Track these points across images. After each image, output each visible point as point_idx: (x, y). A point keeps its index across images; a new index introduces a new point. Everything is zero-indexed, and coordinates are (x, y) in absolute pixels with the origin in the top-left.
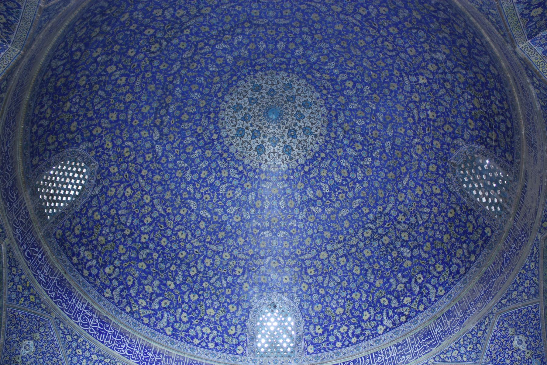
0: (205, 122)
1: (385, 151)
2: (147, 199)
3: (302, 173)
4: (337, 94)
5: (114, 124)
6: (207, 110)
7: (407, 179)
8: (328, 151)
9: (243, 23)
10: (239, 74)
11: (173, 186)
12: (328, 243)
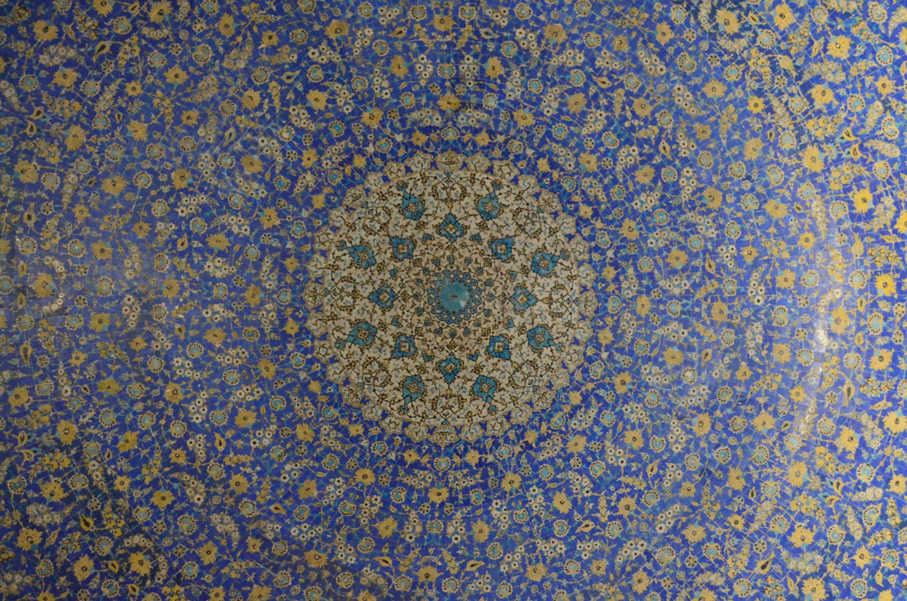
3: (599, 224)
4: (357, 129)
6: (389, 469)
8: (530, 152)
9: (132, 353)
10: (303, 375)
12: (775, 145)
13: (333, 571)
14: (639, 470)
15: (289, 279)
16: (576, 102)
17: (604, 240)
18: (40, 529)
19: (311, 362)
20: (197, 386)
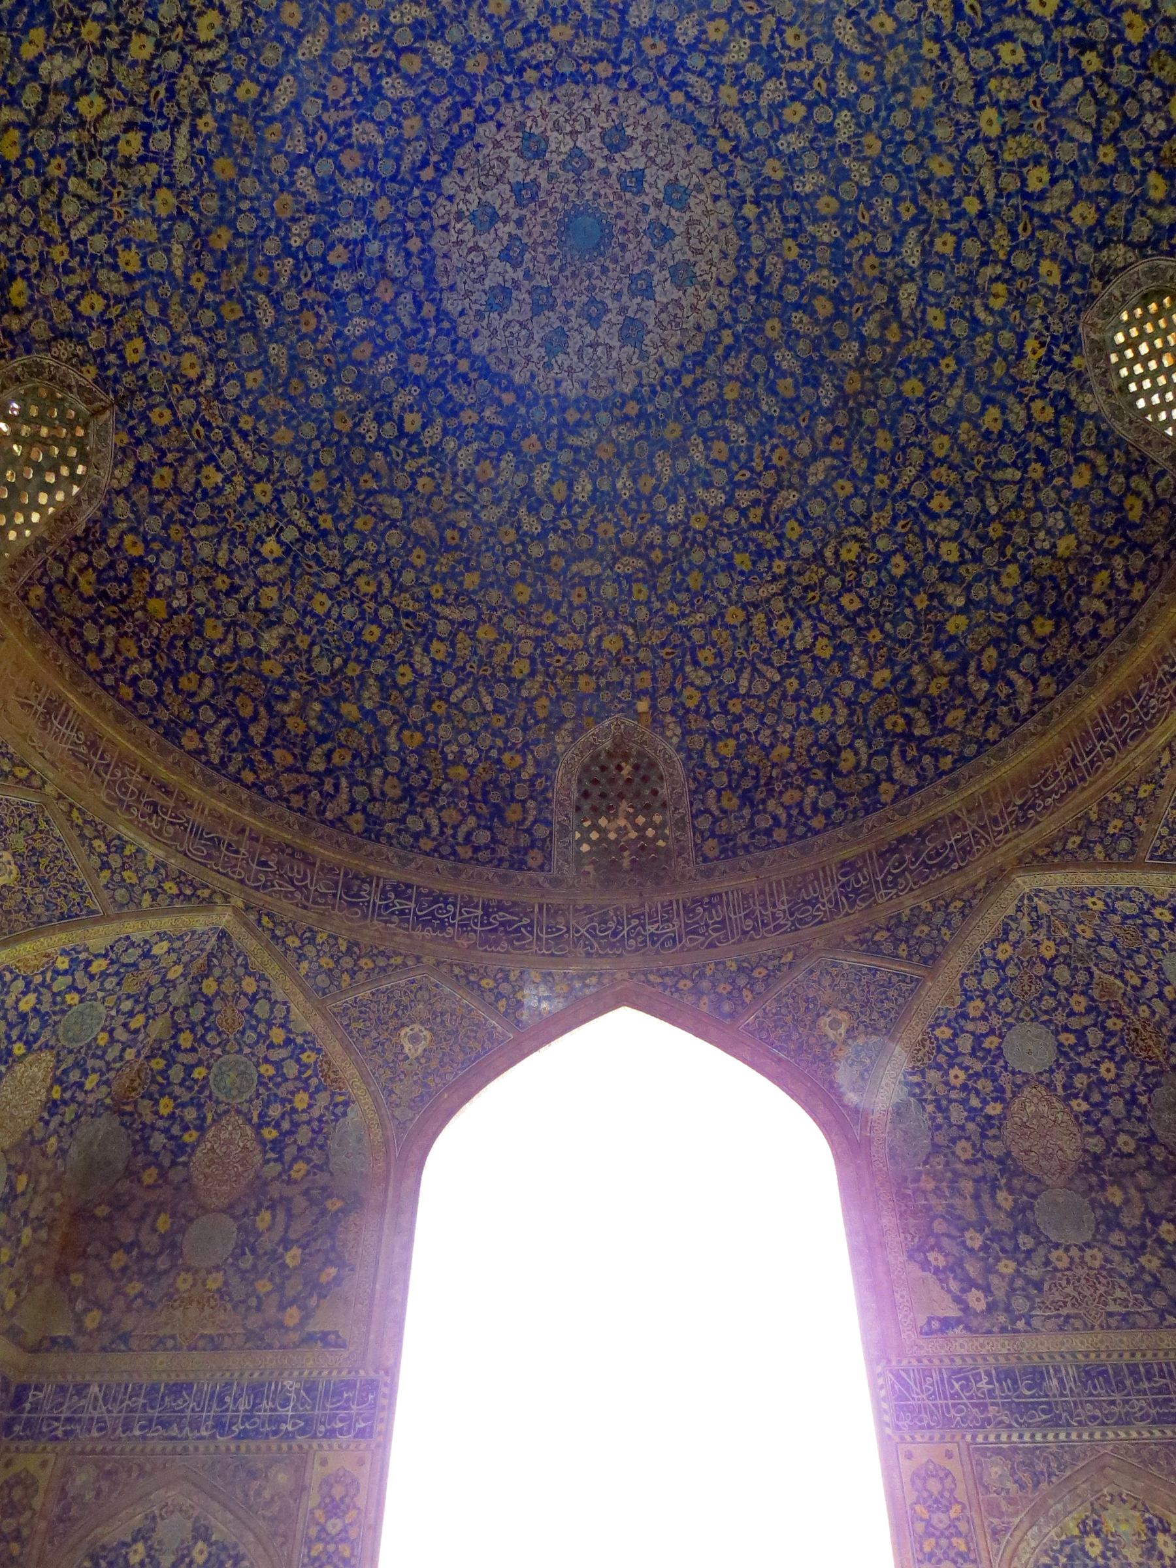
0: (775, 267)
1: (267, 292)
2: (990, 122)
3: (479, 98)
4: (433, 376)
5: (999, 395)
6: (765, 302)
7: (177, 262)
8: (416, 192)
9: (666, 562)
11: (900, 118)
13: (865, 366)
14: (753, 24)
15: (587, 416)
16: (351, 160)
17: (495, 89)
18: (816, 638)
19: (663, 386)
20: (692, 499)
